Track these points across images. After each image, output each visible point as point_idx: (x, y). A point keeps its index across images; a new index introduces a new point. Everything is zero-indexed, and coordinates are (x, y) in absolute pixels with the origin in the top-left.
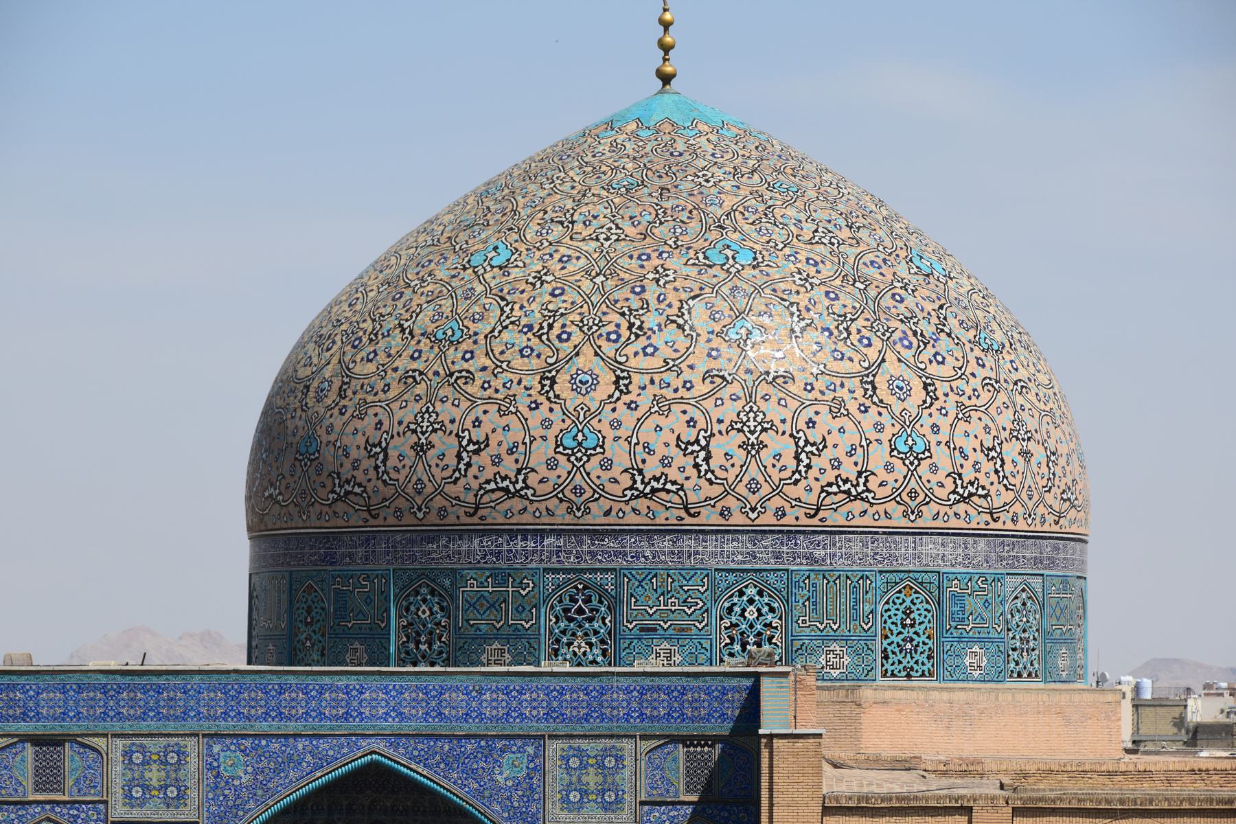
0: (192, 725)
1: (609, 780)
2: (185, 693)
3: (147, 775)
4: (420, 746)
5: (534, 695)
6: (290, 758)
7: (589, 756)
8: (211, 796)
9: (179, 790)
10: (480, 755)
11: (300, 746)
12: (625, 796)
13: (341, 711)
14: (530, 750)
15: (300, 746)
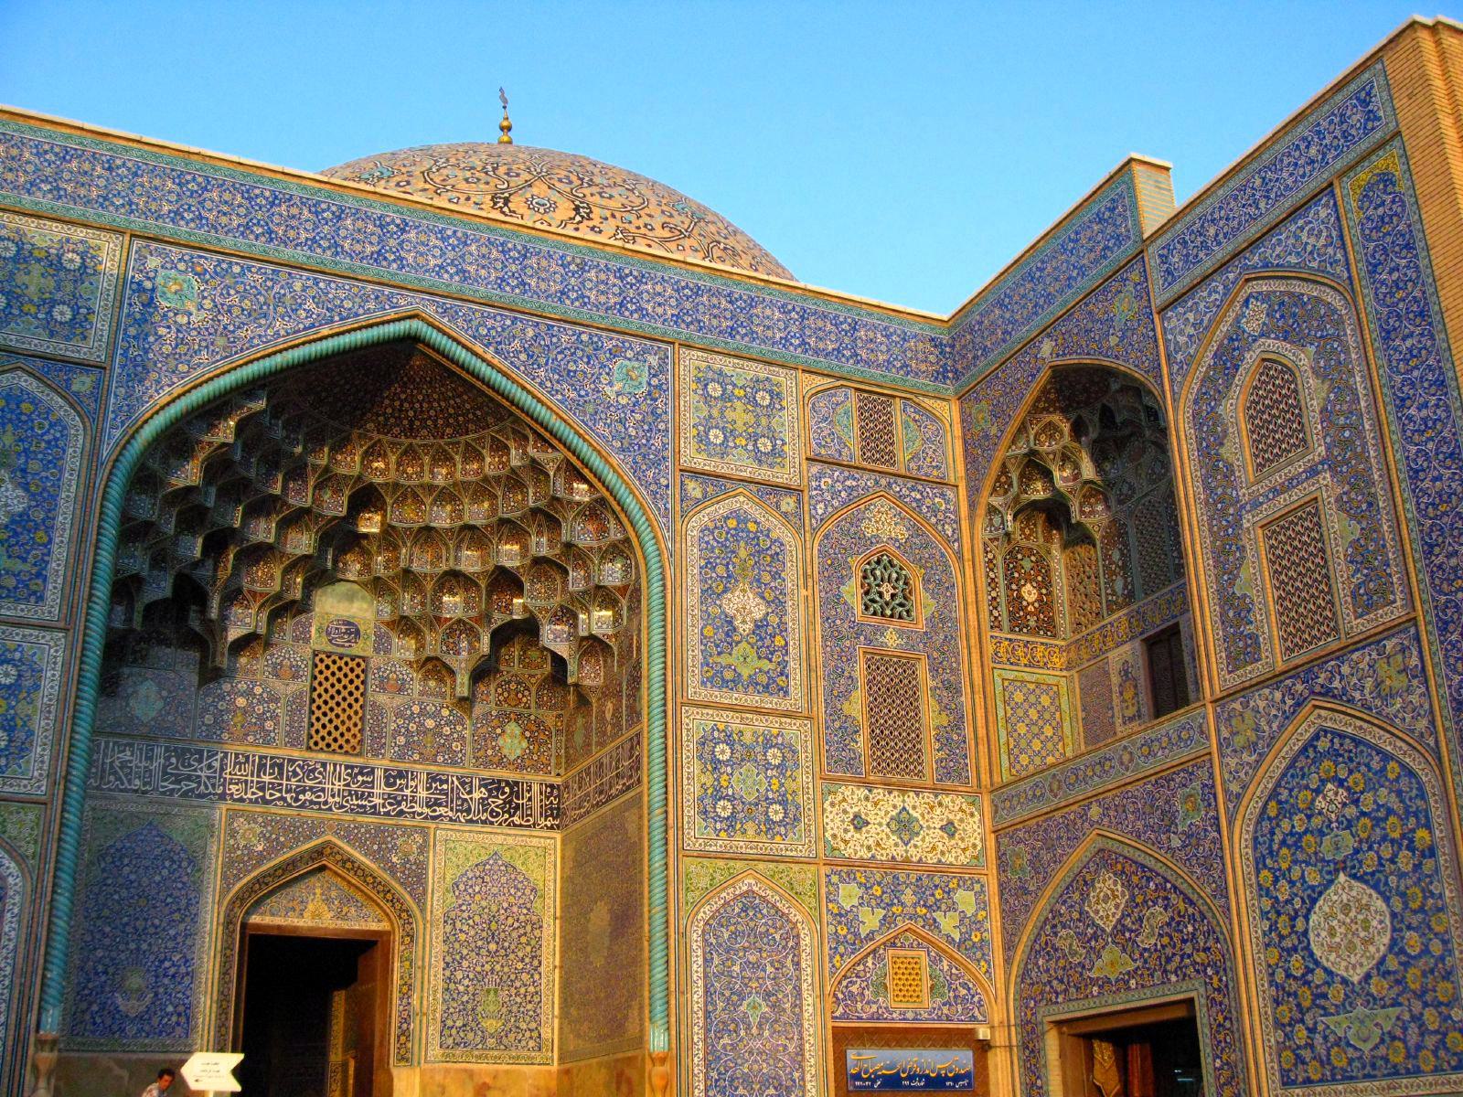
0: (120, 219)
1: (764, 421)
2: (110, 169)
3: (21, 278)
4: (490, 323)
5: (659, 288)
6: (280, 299)
7: (735, 385)
8: (132, 331)
9: (76, 313)
10: (580, 353)
11: (298, 286)
12: (786, 448)
13: (369, 249)
14: (653, 360)
15: (298, 286)
